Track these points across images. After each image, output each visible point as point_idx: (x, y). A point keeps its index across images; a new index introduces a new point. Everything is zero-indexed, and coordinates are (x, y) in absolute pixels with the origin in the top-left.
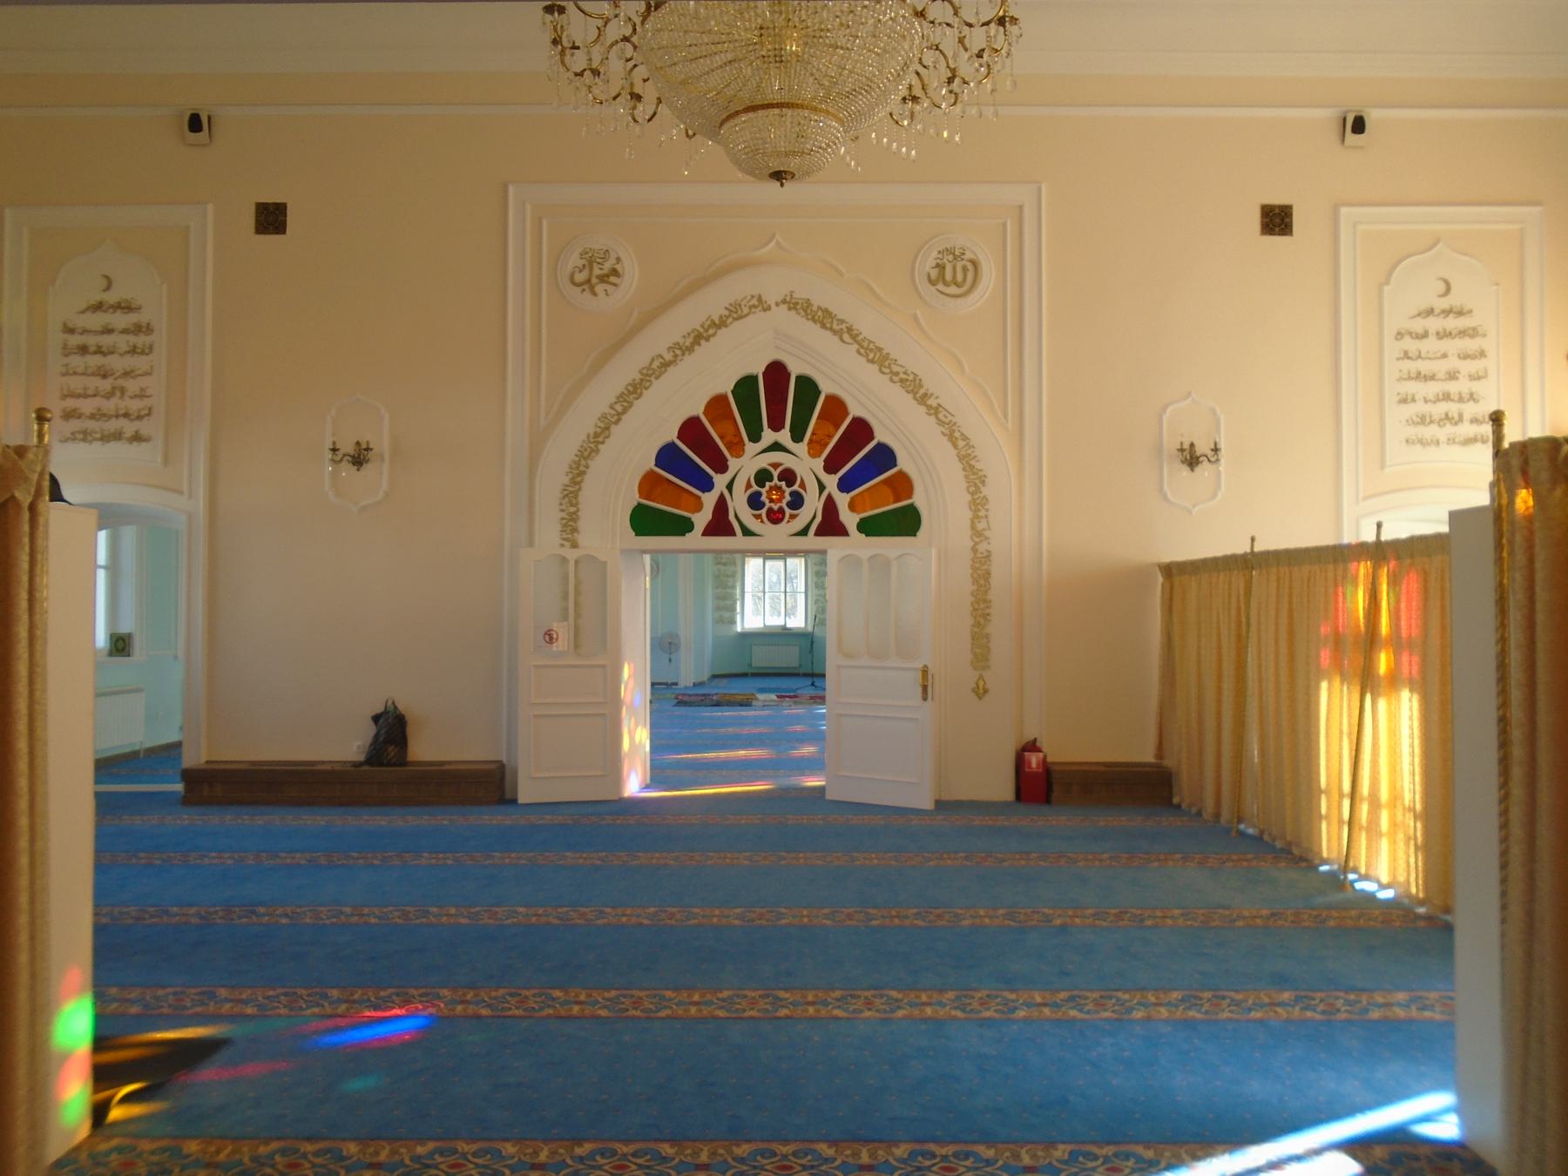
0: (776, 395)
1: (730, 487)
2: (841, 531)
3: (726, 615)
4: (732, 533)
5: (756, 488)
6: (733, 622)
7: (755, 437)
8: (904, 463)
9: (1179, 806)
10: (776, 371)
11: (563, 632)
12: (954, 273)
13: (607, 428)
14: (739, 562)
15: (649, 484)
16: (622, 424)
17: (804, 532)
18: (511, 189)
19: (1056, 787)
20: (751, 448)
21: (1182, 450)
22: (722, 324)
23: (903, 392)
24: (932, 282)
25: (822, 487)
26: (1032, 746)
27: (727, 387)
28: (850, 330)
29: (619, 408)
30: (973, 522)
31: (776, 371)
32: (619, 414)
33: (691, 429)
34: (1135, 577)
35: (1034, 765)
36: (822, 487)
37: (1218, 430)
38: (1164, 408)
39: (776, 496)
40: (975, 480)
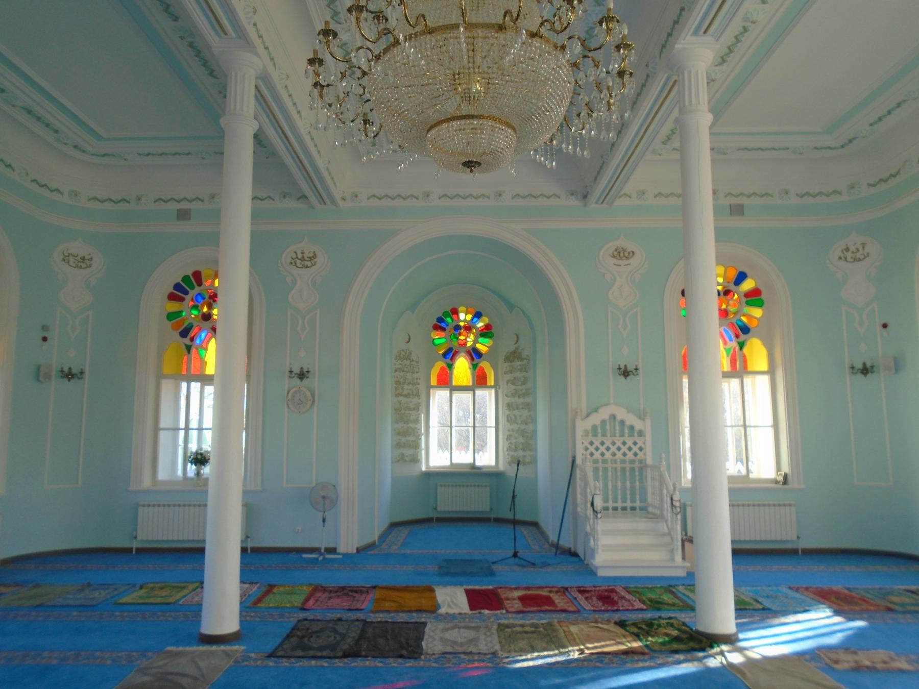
3: (408, 452)
6: (416, 460)
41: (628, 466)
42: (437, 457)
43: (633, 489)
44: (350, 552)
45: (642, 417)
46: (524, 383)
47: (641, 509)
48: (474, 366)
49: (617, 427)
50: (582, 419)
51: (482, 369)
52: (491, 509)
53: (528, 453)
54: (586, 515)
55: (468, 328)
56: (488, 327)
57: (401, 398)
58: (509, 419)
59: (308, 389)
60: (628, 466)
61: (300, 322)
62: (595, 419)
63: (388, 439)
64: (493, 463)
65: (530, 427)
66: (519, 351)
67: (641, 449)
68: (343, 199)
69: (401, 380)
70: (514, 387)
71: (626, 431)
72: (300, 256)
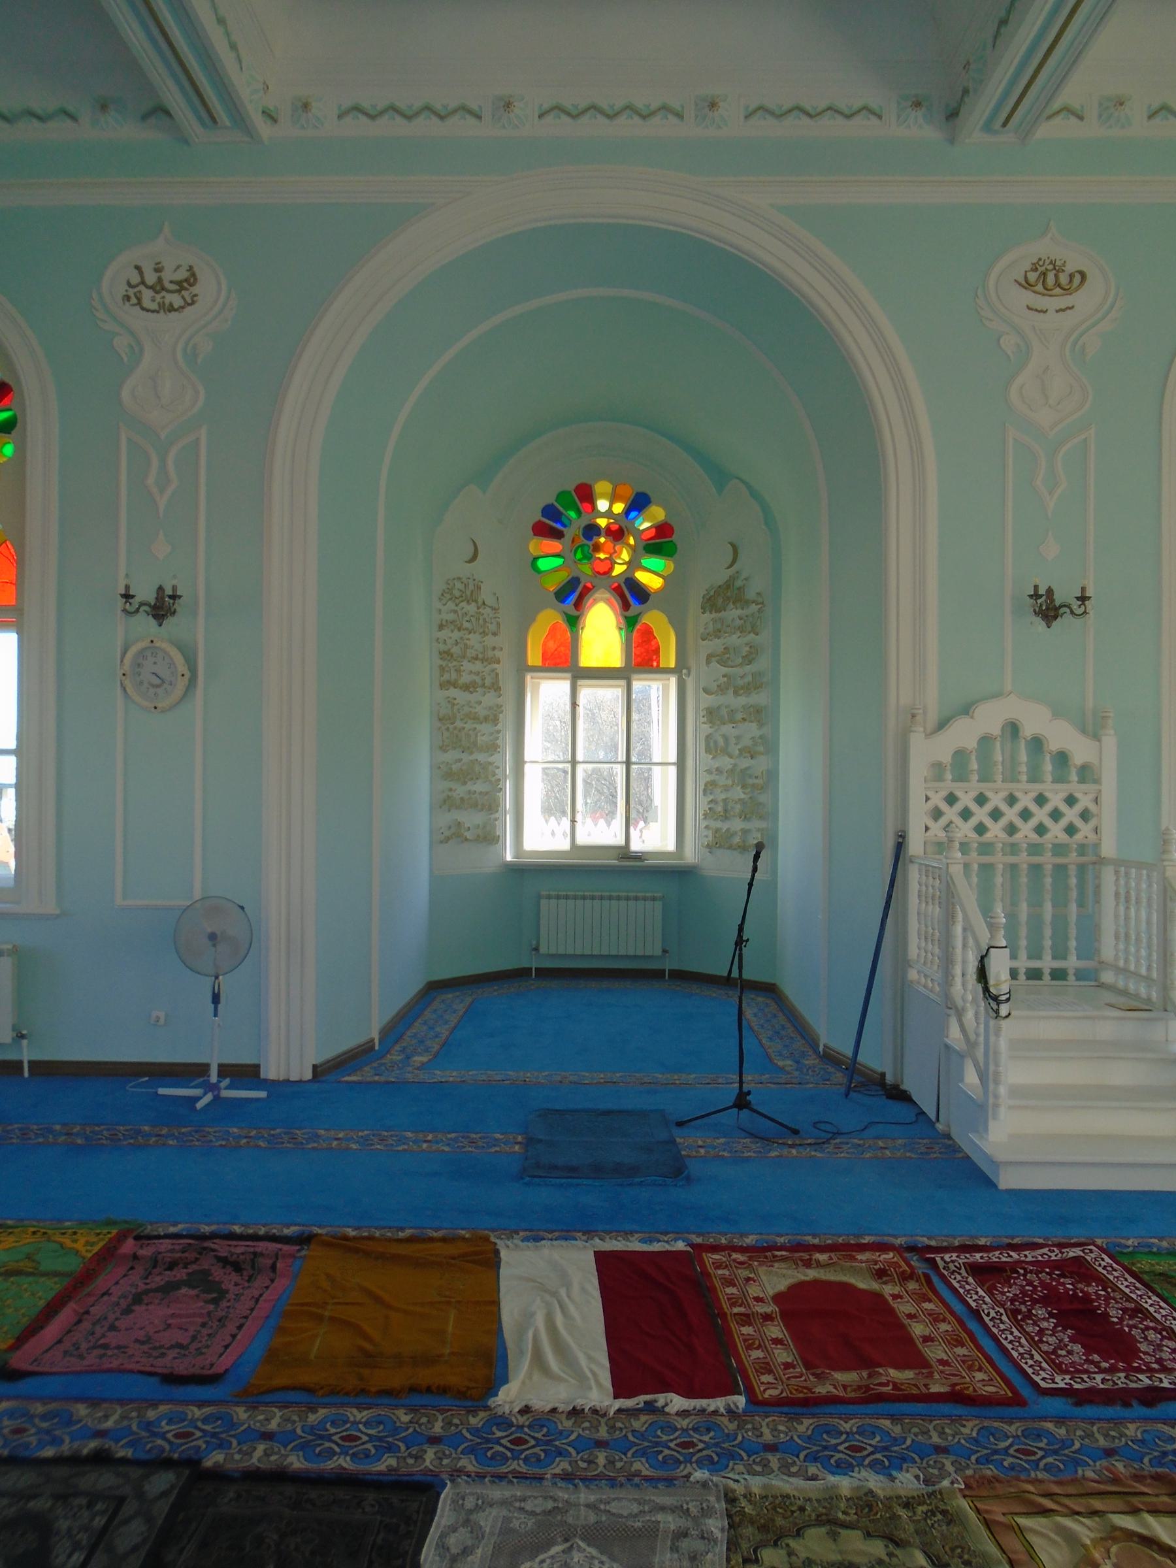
3: (471, 819)
6: (489, 838)
14: (508, 687)
41: (1048, 860)
42: (542, 834)
43: (1060, 922)
44: (294, 1077)
45: (1092, 728)
46: (749, 659)
47: (1081, 975)
48: (629, 622)
49: (1023, 757)
50: (929, 735)
51: (647, 635)
52: (665, 951)
53: (757, 824)
54: (947, 996)
55: (617, 534)
56: (663, 530)
57: (453, 692)
58: (711, 746)
59: (181, 648)
60: (1048, 860)
61: (155, 463)
62: (962, 736)
64: (670, 846)
65: (761, 764)
66: (739, 583)
67: (1085, 815)
68: (270, 116)
69: (456, 650)
70: (725, 670)
71: (1048, 767)
72: (151, 278)
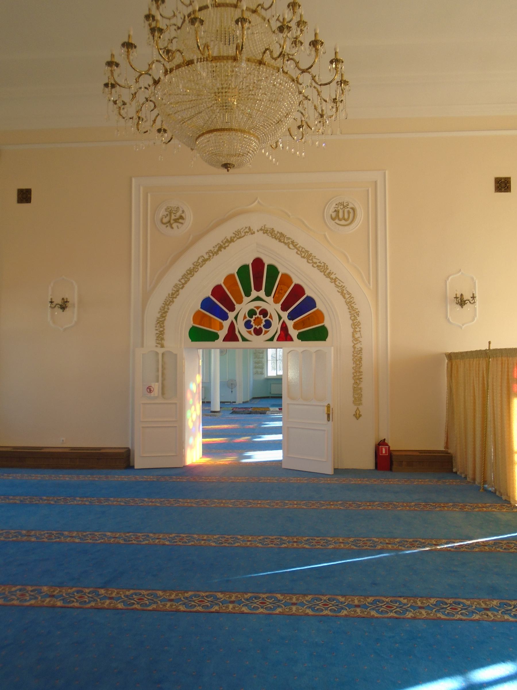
0: (259, 274)
1: (236, 318)
2: (291, 339)
3: (259, 370)
4: (237, 340)
5: (248, 318)
6: (262, 373)
7: (248, 294)
8: (320, 306)
9: (456, 473)
10: (258, 263)
11: (156, 387)
12: (343, 214)
13: (178, 291)
15: (197, 317)
16: (184, 288)
17: (272, 339)
18: (133, 180)
19: (394, 463)
20: (246, 299)
21: (456, 298)
22: (232, 240)
23: (319, 271)
24: (333, 219)
25: (280, 318)
26: (382, 443)
27: (234, 270)
28: (293, 242)
29: (183, 281)
30: (353, 333)
31: (258, 263)
32: (183, 284)
33: (218, 291)
34: (433, 360)
35: (384, 452)
36: (280, 318)
37: (475, 289)
38: (448, 278)
39: (258, 322)
40: (354, 314)
63: (251, 365)
